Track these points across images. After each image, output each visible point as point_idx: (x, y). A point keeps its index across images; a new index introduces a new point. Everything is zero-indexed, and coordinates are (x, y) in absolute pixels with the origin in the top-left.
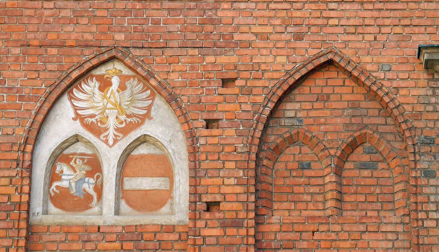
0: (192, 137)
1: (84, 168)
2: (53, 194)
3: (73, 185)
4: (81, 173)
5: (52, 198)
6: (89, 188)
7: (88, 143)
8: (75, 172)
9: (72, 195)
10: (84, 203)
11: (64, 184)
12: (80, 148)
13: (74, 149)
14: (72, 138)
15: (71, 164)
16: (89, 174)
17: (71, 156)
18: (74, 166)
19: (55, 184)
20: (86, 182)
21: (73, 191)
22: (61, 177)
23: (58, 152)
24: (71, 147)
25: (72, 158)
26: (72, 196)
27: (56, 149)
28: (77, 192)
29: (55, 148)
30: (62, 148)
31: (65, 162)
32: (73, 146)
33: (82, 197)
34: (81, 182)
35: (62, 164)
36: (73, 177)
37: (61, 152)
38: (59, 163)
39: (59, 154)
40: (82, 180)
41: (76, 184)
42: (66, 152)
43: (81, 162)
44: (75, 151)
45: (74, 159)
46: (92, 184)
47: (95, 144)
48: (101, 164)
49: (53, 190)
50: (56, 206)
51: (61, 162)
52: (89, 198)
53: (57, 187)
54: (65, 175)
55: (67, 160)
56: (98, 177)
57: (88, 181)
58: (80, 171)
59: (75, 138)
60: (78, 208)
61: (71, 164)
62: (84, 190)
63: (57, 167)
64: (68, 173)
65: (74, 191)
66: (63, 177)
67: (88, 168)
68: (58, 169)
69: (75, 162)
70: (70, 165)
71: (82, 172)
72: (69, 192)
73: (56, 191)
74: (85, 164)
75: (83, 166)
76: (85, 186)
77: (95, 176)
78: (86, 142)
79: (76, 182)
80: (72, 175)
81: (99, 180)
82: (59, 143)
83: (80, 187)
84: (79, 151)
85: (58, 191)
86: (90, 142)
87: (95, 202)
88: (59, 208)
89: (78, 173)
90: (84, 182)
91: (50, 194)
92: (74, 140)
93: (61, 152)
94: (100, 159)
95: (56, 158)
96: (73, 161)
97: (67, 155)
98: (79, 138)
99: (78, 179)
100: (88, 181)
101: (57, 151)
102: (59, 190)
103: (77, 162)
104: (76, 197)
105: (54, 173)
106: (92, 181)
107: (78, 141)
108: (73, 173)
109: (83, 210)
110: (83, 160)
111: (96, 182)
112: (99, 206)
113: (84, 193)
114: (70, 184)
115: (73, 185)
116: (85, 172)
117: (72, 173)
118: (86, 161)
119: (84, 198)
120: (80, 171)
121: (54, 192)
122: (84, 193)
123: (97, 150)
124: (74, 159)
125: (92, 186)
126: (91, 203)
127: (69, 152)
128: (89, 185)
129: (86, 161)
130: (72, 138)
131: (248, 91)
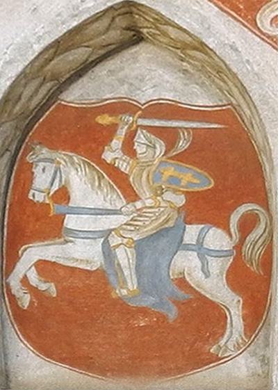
1: (173, 180)
2: (25, 300)
3: (125, 257)
4: (156, 206)
5: (22, 318)
6: (207, 275)
7: (191, 51)
8: (131, 195)
9: (120, 304)
11: (81, 253)
12: (147, 76)
13: (122, 82)
14: (106, 22)
15: (108, 156)
16: (205, 208)
17: (105, 120)
18: (124, 167)
19: (32, 254)
20: (188, 248)
21: (128, 286)
22: (60, 219)
23: (33, 95)
24: (101, 71)
25: (112, 130)
26: (123, 309)
27: (24, 78)
28: (143, 290)
29: (13, 72)
30: (54, 77)
31: (74, 149)
32: (111, 64)
33: (172, 314)
34: (163, 243)
35: (61, 156)
36: (123, 219)
37: (52, 97)
38: (45, 152)
39: (42, 108)
40: (164, 239)
41: (140, 255)
42: (75, 96)
43: (160, 147)
44: (122, 92)
45: (122, 132)
46: (219, 254)
47: (231, 59)
48: (263, 158)
49: (25, 281)
50: (46, 350)
51: (53, 146)
52: (202, 318)
53: (44, 267)
54: (79, 211)
55: (86, 136)
56: (247, 225)
57: (200, 242)
58: (158, 192)
59: (121, 22)
60: (154, 363)
61: (108, 156)
62: (182, 282)
63: (37, 171)
64: (97, 200)
65: (132, 284)
66: (71, 222)
67: (195, 179)
68: (42, 184)
69: (129, 148)
70: (102, 163)
71: (168, 196)
72: (107, 293)
73: (43, 287)
74: (180, 158)
75: (170, 171)
76: (187, 263)
77: (234, 219)
78: (185, 47)
79: (140, 248)
80: (115, 212)
81: (252, 237)
82: (38, 48)
83: (158, 266)
84: (146, 95)
85: (51, 288)
86: (202, 47)
87: (236, 336)
88: (62, 360)
89: (149, 202)
90: (181, 245)
91: (13, 299)
92: (115, 35)
93: (52, 97)
94: (259, 137)
95: (29, 127)
96: (117, 143)
97: (85, 114)
98: (141, 22)
99: (150, 229)
100: (200, 242)
101: (27, 93)
102: (57, 282)
103: (140, 149)
104: (144, 311)
105: (22, 200)
106: (217, 239)
107: (137, 38)
108: (120, 202)
109: (180, 370)
110: (169, 137)
111: (239, 247)
112: (254, 354)
113: (181, 294)
114: (108, 252)
115: (125, 257)
116: (180, 200)
117: (116, 200)
118: (183, 145)
119: (183, 317)
120: (158, 192)
121: (34, 291)
122: (181, 294)
123: (244, 91)
124: (122, 132)
125: (218, 266)
126: (216, 341)
127: (94, 98)
128: (202, 257)
129: (183, 145)
130: (106, 22)
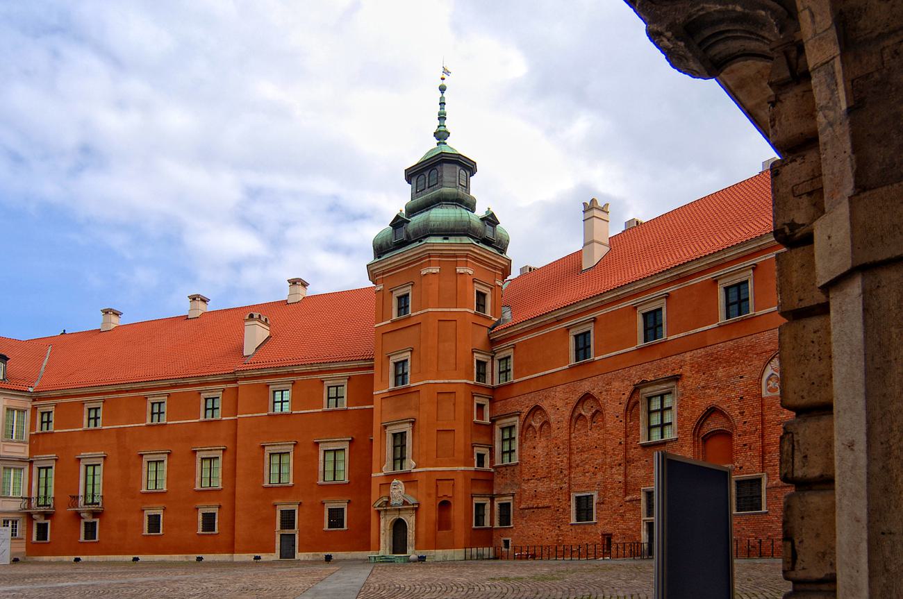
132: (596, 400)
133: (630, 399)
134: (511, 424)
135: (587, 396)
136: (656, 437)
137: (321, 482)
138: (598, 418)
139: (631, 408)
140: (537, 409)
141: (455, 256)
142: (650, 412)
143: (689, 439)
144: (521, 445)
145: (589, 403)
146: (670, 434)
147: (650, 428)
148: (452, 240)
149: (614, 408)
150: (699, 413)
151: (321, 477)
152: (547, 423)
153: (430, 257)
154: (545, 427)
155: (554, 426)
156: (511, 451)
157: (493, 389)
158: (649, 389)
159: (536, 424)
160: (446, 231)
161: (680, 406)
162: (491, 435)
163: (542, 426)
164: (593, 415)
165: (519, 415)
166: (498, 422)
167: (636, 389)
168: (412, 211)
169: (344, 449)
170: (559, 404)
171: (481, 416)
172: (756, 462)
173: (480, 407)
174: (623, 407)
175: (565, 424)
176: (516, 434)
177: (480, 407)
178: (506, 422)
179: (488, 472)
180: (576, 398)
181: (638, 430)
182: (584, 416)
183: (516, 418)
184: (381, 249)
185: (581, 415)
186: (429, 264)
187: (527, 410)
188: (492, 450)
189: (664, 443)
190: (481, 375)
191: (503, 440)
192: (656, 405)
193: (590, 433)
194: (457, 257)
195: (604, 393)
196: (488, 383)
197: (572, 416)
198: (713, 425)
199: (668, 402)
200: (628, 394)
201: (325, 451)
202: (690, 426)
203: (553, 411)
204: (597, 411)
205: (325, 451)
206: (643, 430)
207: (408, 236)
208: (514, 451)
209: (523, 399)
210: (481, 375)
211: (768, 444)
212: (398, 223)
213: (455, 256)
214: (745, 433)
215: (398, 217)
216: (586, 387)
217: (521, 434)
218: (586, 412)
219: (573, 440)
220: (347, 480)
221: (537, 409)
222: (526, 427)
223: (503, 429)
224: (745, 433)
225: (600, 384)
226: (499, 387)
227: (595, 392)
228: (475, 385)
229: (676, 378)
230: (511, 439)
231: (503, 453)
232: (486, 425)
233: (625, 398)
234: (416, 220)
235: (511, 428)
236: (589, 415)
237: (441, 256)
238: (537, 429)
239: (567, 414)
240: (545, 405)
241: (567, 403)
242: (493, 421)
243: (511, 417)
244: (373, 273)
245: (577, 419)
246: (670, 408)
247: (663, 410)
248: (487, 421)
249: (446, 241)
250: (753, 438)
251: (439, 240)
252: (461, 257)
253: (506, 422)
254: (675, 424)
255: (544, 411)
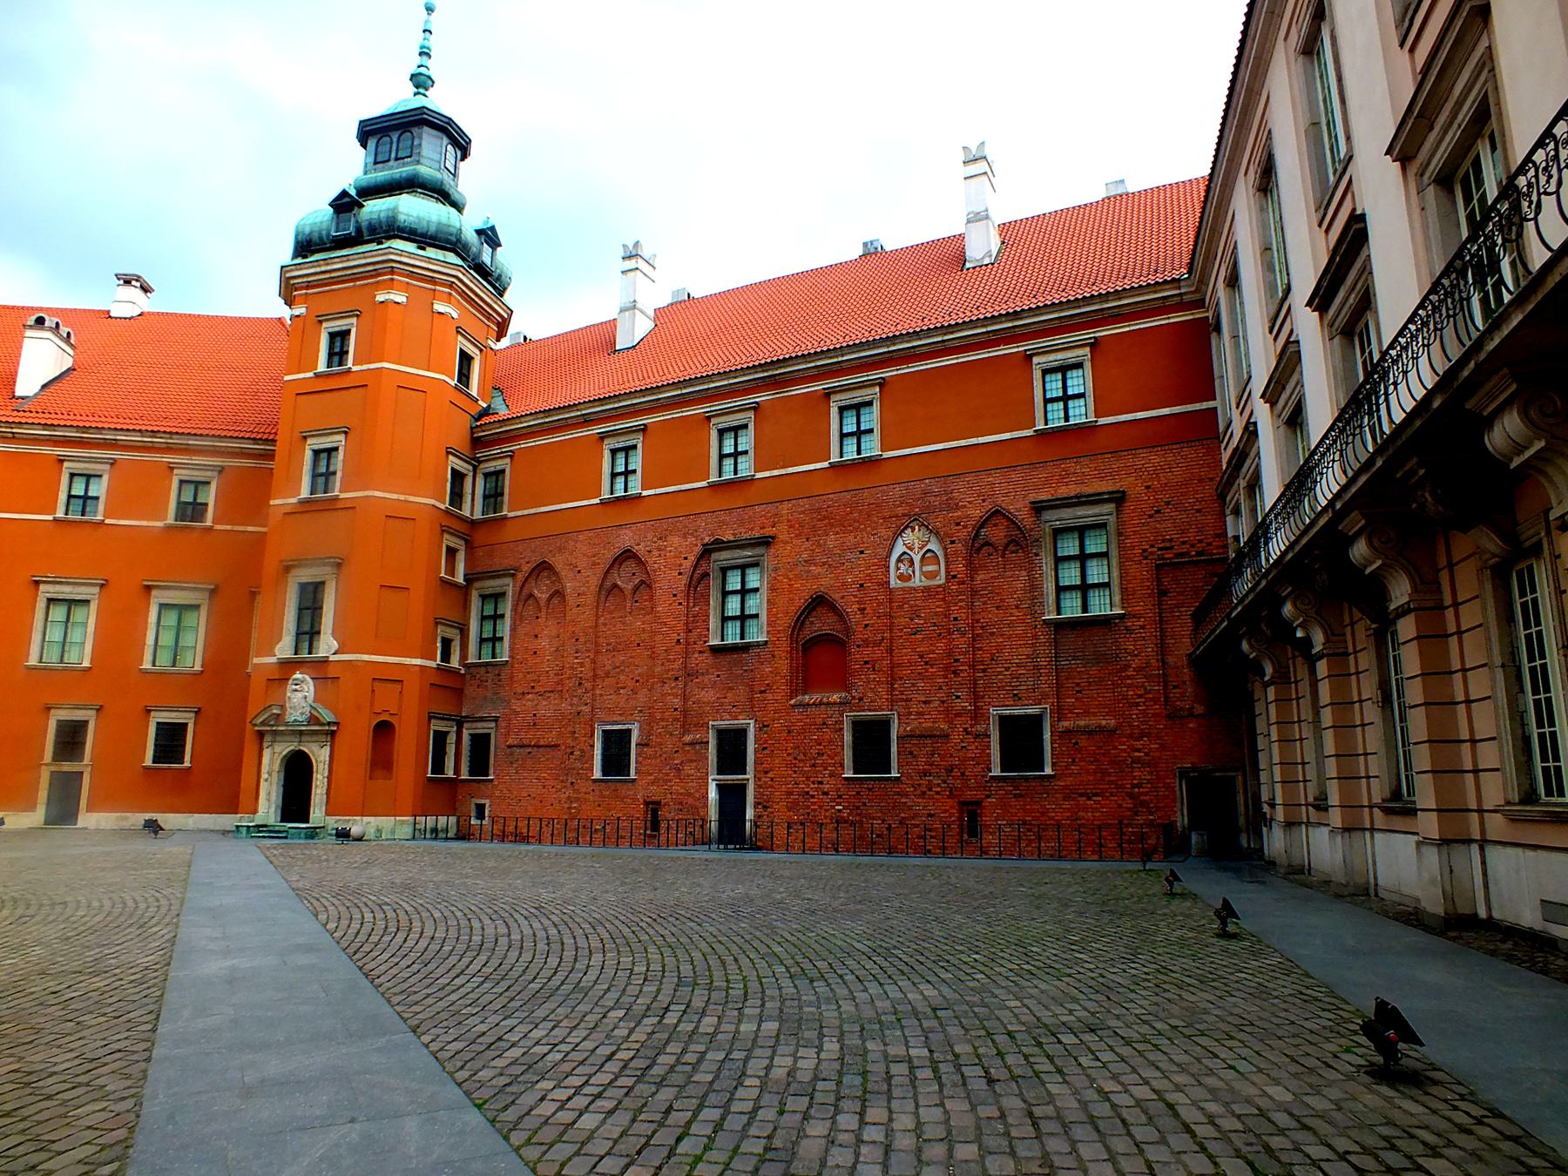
0: (945, 549)
10: (909, 578)
131: (965, 527)
132: (640, 562)
133: (695, 567)
134: (498, 590)
135: (628, 555)
136: (733, 637)
137: (147, 665)
138: (643, 593)
139: (697, 582)
140: (544, 567)
141: (432, 281)
142: (725, 594)
143: (784, 645)
144: (513, 630)
145: (630, 566)
146: (756, 634)
147: (725, 619)
148: (431, 252)
149: (670, 579)
150: (800, 602)
151: (148, 657)
152: (559, 594)
153: (392, 273)
154: (555, 601)
155: (571, 601)
156: (495, 639)
157: (473, 524)
158: (724, 555)
159: (542, 594)
160: (424, 235)
161: (772, 589)
162: (466, 606)
163: (552, 596)
164: (636, 589)
165: (513, 575)
166: (477, 585)
167: (706, 552)
168: (369, 192)
169: (197, 607)
170: (582, 563)
171: (451, 570)
172: (882, 690)
173: (452, 552)
174: (684, 580)
175: (590, 599)
176: (507, 608)
177: (452, 552)
178: (492, 585)
179: (455, 672)
180: (609, 555)
181: (707, 621)
182: (621, 590)
183: (509, 581)
184: (305, 247)
185: (615, 586)
186: (390, 285)
187: (526, 568)
188: (464, 632)
189: (746, 648)
190: (457, 497)
191: (483, 618)
192: (734, 582)
193: (629, 619)
194: (435, 283)
195: (656, 553)
196: (466, 512)
197: (601, 586)
198: (821, 624)
199: (754, 579)
200: (692, 558)
201: (162, 606)
202: (785, 622)
203: (571, 575)
204: (642, 582)
205: (162, 606)
206: (714, 622)
207: (359, 230)
208: (501, 639)
209: (520, 549)
210: (457, 497)
211: (899, 665)
212: (344, 204)
213: (432, 281)
214: (866, 643)
215: (344, 194)
216: (626, 539)
217: (515, 609)
218: (625, 579)
219: (602, 628)
220: (198, 668)
221: (544, 567)
222: (524, 598)
223: (484, 597)
224: (866, 643)
225: (650, 536)
226: (484, 521)
227: (640, 549)
228: (447, 512)
229: (766, 542)
230: (497, 617)
231: (482, 641)
232: (455, 585)
233: (688, 564)
234: (375, 208)
235: (498, 597)
236: (630, 586)
237: (411, 275)
238: (542, 604)
239: (594, 581)
240: (558, 562)
241: (594, 564)
242: (470, 579)
243: (499, 577)
244: (289, 290)
245: (609, 592)
246: (756, 590)
247: (744, 592)
248: (460, 579)
249: (421, 252)
250: (879, 652)
251: (411, 247)
252: (442, 285)
253: (492, 585)
254: (764, 618)
255: (556, 574)
